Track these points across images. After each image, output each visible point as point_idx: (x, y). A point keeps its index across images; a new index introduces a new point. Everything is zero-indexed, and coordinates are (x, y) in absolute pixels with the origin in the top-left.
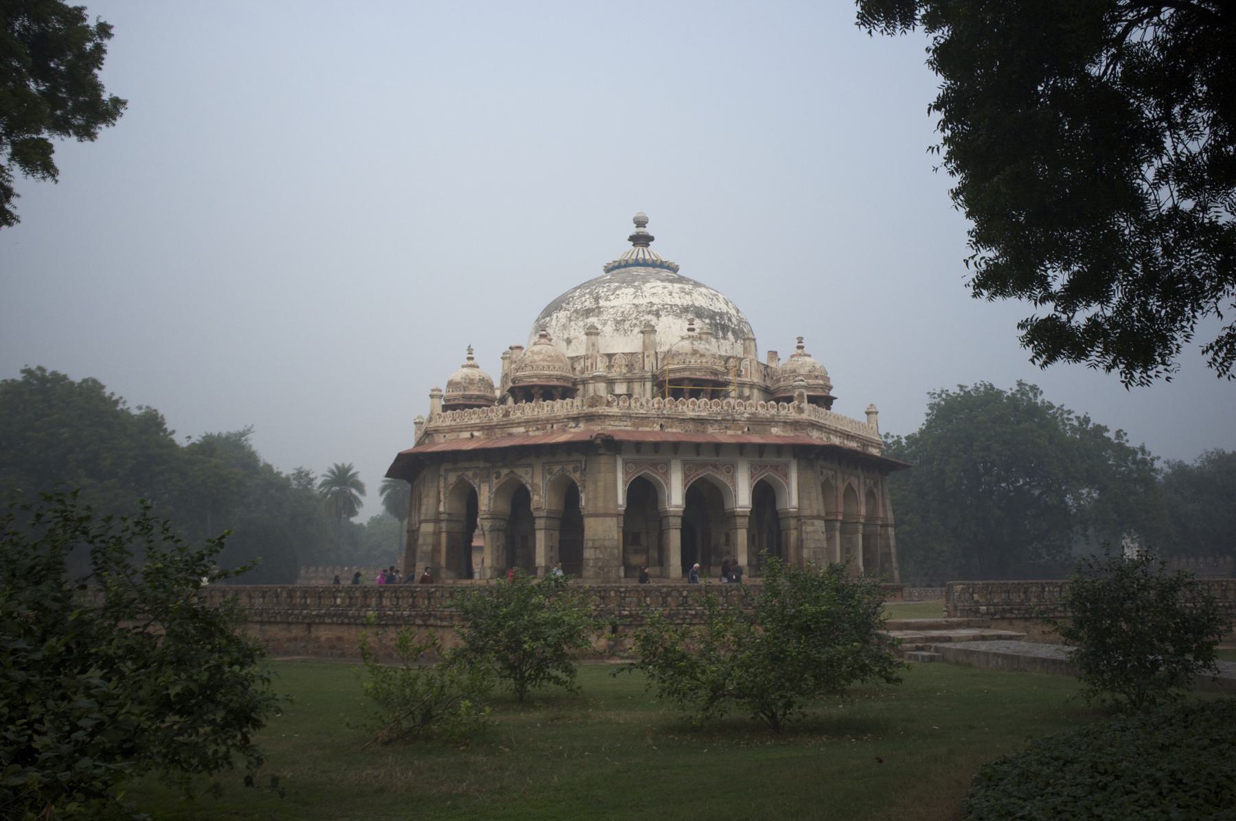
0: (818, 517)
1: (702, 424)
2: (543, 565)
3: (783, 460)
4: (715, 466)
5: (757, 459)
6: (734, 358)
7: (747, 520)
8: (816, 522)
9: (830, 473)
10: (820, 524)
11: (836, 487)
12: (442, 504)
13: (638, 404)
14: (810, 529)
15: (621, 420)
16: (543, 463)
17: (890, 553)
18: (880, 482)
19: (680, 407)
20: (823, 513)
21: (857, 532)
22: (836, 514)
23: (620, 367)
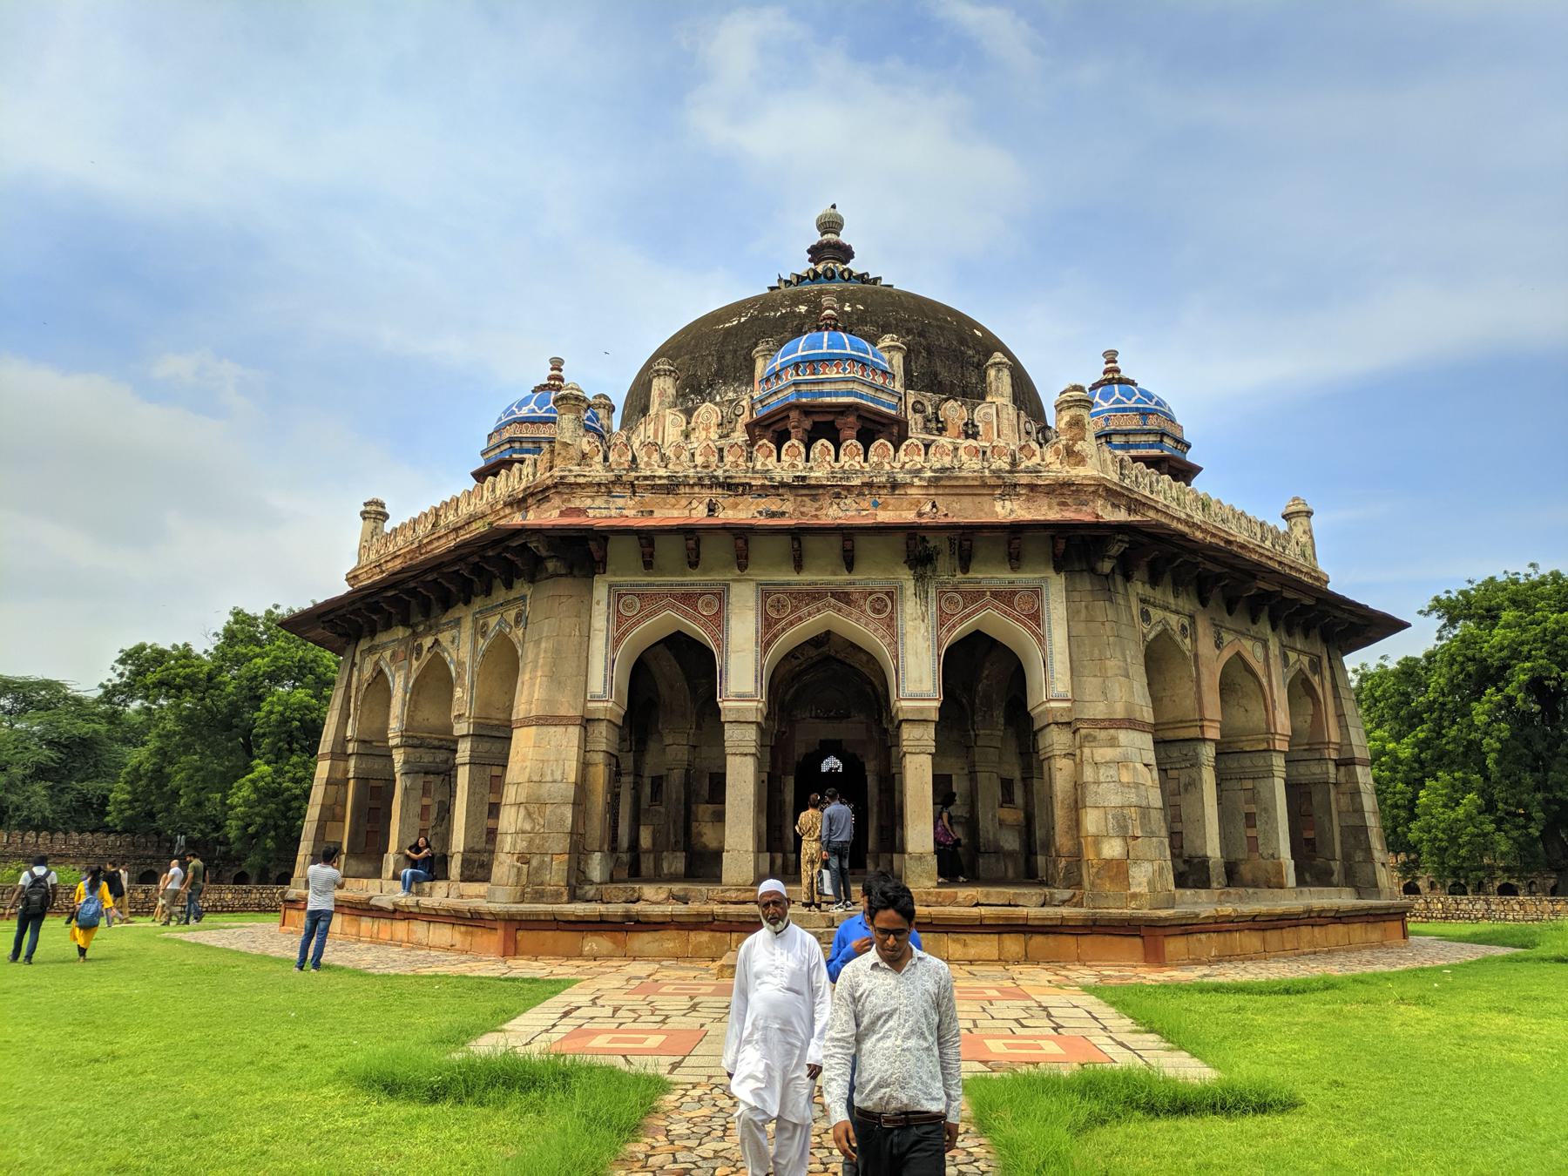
0: (1131, 724)
1: (814, 498)
2: (462, 849)
3: (1025, 577)
4: (844, 597)
5: (959, 576)
7: (930, 732)
8: (1124, 736)
9: (1174, 620)
10: (1139, 745)
11: (1196, 656)
12: (350, 721)
13: (656, 457)
16: (474, 615)
17: (1364, 829)
18: (1325, 663)
20: (1148, 716)
21: (1270, 774)
23: (707, 429)
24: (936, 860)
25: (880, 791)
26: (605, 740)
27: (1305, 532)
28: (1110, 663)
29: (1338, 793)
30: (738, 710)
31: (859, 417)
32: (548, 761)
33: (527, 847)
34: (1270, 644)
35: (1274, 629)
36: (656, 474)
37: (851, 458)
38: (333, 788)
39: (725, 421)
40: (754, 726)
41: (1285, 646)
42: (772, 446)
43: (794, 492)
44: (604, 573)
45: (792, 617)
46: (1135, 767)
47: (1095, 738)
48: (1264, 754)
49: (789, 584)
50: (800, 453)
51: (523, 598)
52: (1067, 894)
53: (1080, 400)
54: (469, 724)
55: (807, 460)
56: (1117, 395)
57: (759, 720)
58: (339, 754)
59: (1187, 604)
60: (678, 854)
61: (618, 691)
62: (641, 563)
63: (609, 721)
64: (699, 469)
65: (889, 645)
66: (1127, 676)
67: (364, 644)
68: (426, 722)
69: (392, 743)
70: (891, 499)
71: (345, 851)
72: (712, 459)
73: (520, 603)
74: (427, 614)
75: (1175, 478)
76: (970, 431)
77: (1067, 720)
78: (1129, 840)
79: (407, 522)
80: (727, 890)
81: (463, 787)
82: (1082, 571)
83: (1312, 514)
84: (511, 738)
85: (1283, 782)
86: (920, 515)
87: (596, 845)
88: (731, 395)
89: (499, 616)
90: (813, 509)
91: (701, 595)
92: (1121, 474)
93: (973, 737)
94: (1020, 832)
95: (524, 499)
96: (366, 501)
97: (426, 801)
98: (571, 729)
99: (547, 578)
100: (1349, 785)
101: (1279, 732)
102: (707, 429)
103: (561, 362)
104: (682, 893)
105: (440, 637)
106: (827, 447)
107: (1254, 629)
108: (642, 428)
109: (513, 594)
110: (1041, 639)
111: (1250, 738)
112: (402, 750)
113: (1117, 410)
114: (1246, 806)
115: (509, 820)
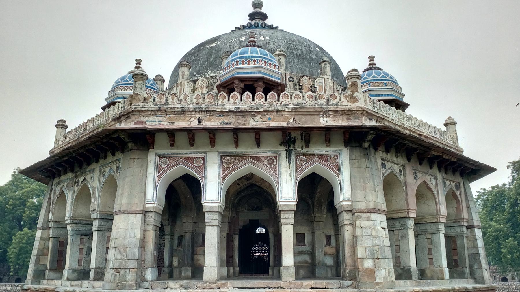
1: (243, 116)
2: (94, 267)
3: (332, 150)
4: (256, 158)
5: (305, 149)
7: (293, 215)
8: (374, 216)
9: (396, 167)
10: (380, 220)
11: (406, 182)
12: (50, 213)
14: (365, 223)
15: (155, 115)
16: (100, 167)
19: (221, 100)
20: (384, 207)
21: (438, 232)
22: (408, 211)
24: (294, 270)
25: (275, 240)
26: (153, 220)
27: (453, 131)
28: (367, 185)
29: (467, 240)
30: (211, 206)
31: (264, 83)
32: (128, 229)
33: (119, 266)
34: (438, 177)
35: (440, 171)
36: (176, 107)
37: (260, 98)
38: (43, 242)
39: (210, 85)
40: (217, 214)
41: (444, 178)
42: (226, 95)
43: (235, 114)
44: (153, 148)
45: (234, 167)
46: (378, 228)
47: (361, 217)
48: (435, 224)
49: (232, 153)
50: (237, 98)
51: (119, 160)
52: (349, 283)
53: (356, 75)
54: (97, 214)
55: (241, 100)
56: (374, 74)
57: (220, 211)
58: (46, 227)
59: (402, 160)
60: (188, 268)
61: (159, 199)
62: (169, 145)
63: (155, 212)
64: (194, 104)
65: (275, 178)
66: (375, 191)
67: (56, 180)
68: (81, 213)
69: (67, 222)
70: (276, 117)
71: (48, 268)
72: (200, 100)
73: (118, 162)
74: (81, 167)
75: (397, 108)
76: (313, 90)
77: (350, 210)
79: (74, 128)
80: (205, 283)
81: (95, 241)
82: (356, 147)
83: (456, 124)
84: (113, 220)
85: (443, 235)
86: (288, 123)
87: (149, 265)
88: (213, 74)
89: (110, 167)
90: (243, 121)
91: (195, 158)
92: (373, 106)
93: (313, 218)
94: (334, 257)
95: (120, 118)
96: (58, 120)
97: (81, 247)
98: (138, 215)
99: (129, 151)
101: (442, 214)
102: (202, 89)
103: (141, 61)
104: (186, 285)
105: (86, 177)
106: (249, 95)
107: (431, 171)
108: (175, 88)
109: (115, 158)
110: (339, 175)
111: (429, 217)
112: (71, 225)
113: (374, 80)
114: (428, 246)
115: (111, 254)
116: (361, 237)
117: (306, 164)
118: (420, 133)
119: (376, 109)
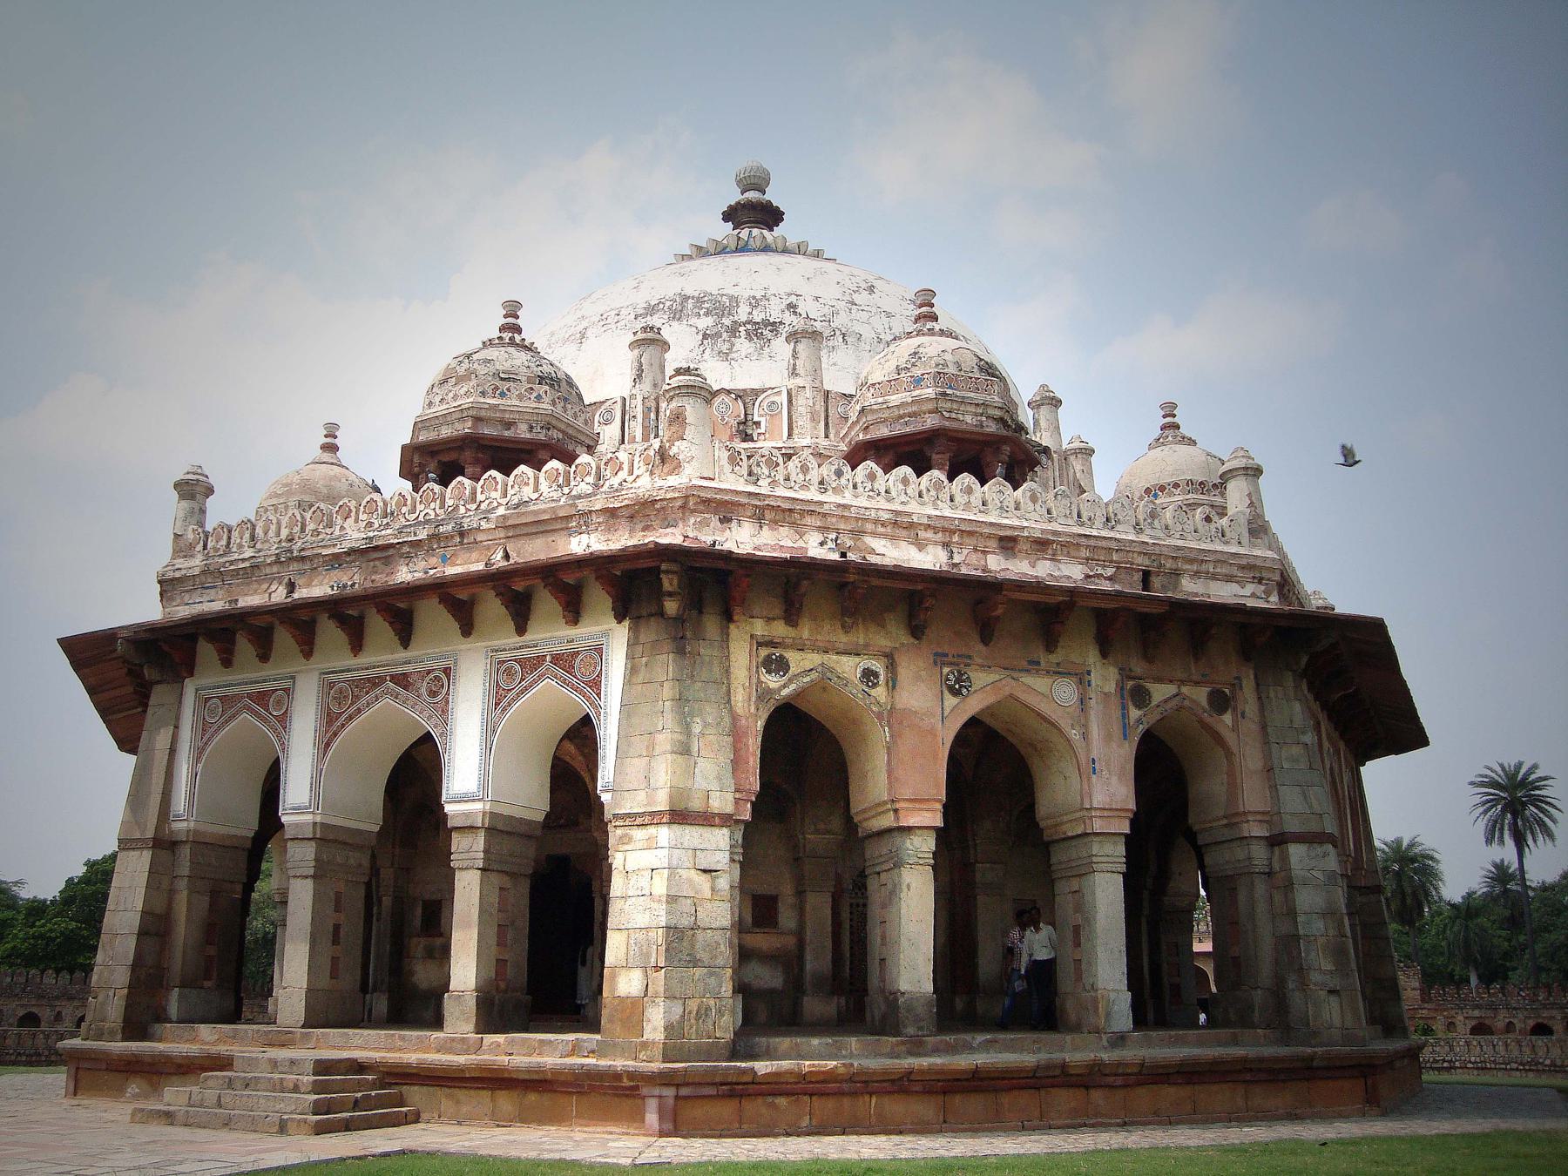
3: (583, 633)
4: (402, 680)
5: (516, 640)
6: (729, 392)
8: (664, 834)
21: (1085, 870)
28: (660, 737)
34: (1095, 678)
35: (1104, 654)
40: (313, 843)
44: (191, 674)
45: (355, 707)
47: (630, 839)
78: (649, 972)
87: (178, 982)
98: (145, 852)
100: (1283, 874)
116: (623, 901)
117: (520, 683)
118: (1002, 533)
119: (764, 483)
